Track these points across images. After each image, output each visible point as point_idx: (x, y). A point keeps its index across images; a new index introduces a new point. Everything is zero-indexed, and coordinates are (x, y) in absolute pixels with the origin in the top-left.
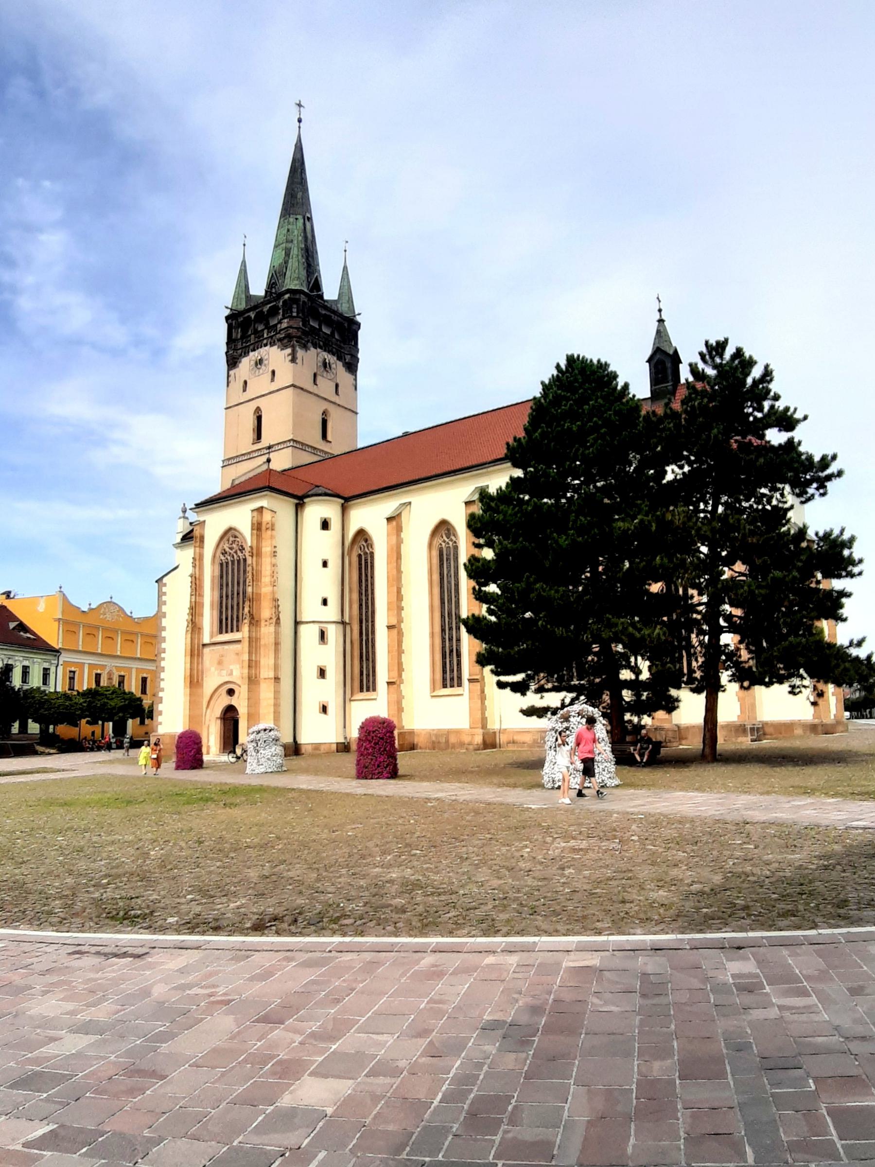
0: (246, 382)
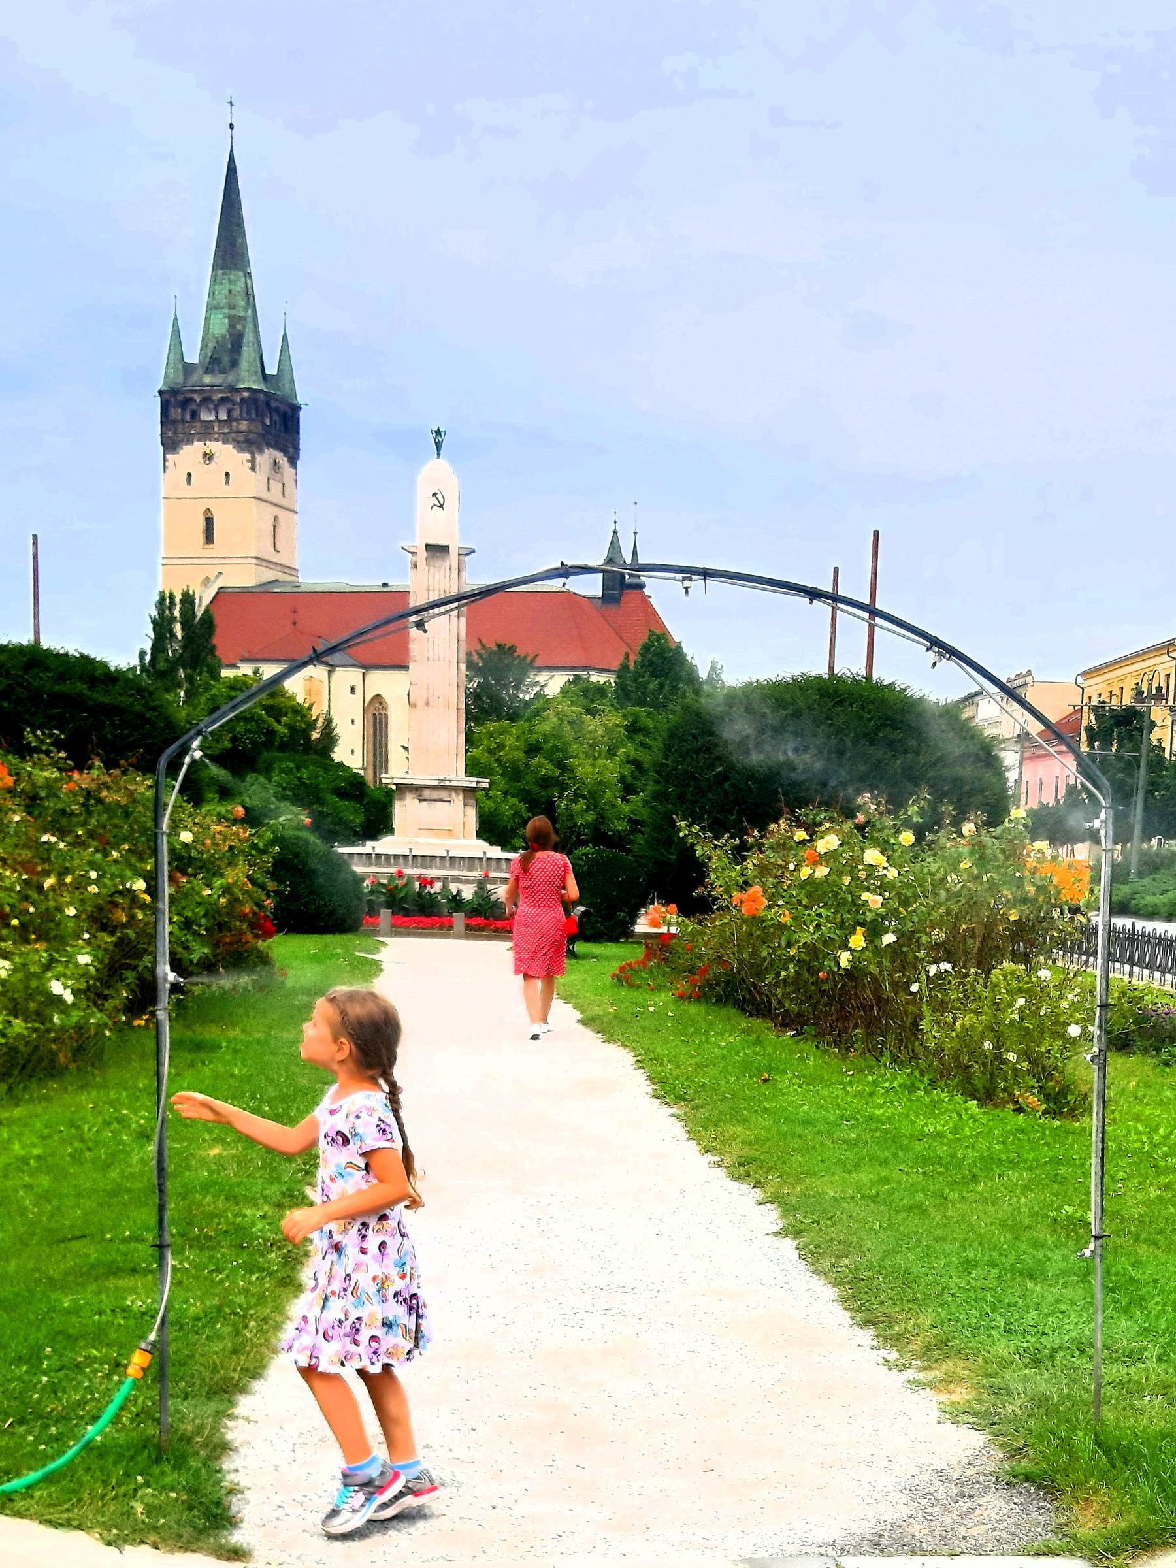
0: (189, 475)
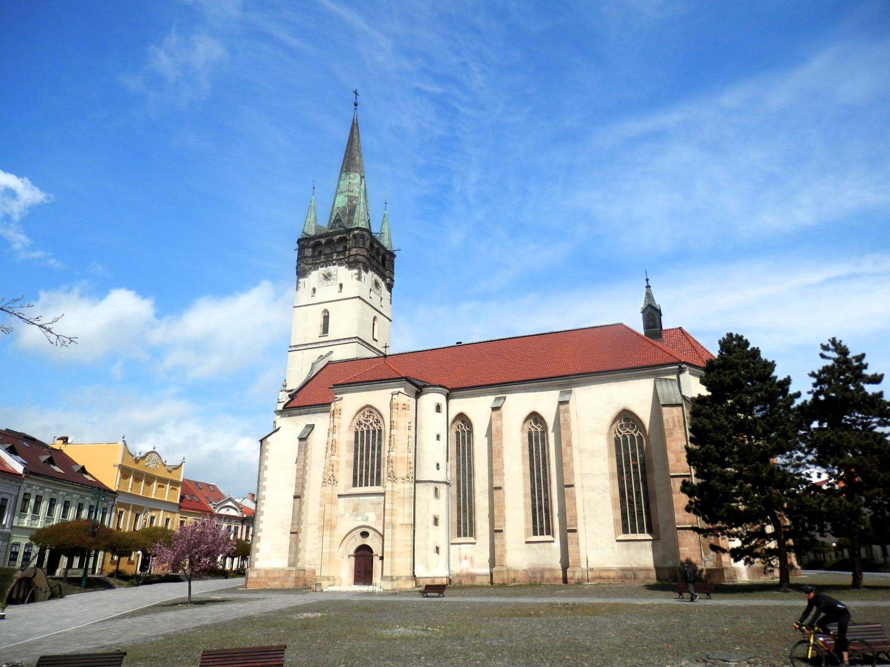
0: (314, 290)
